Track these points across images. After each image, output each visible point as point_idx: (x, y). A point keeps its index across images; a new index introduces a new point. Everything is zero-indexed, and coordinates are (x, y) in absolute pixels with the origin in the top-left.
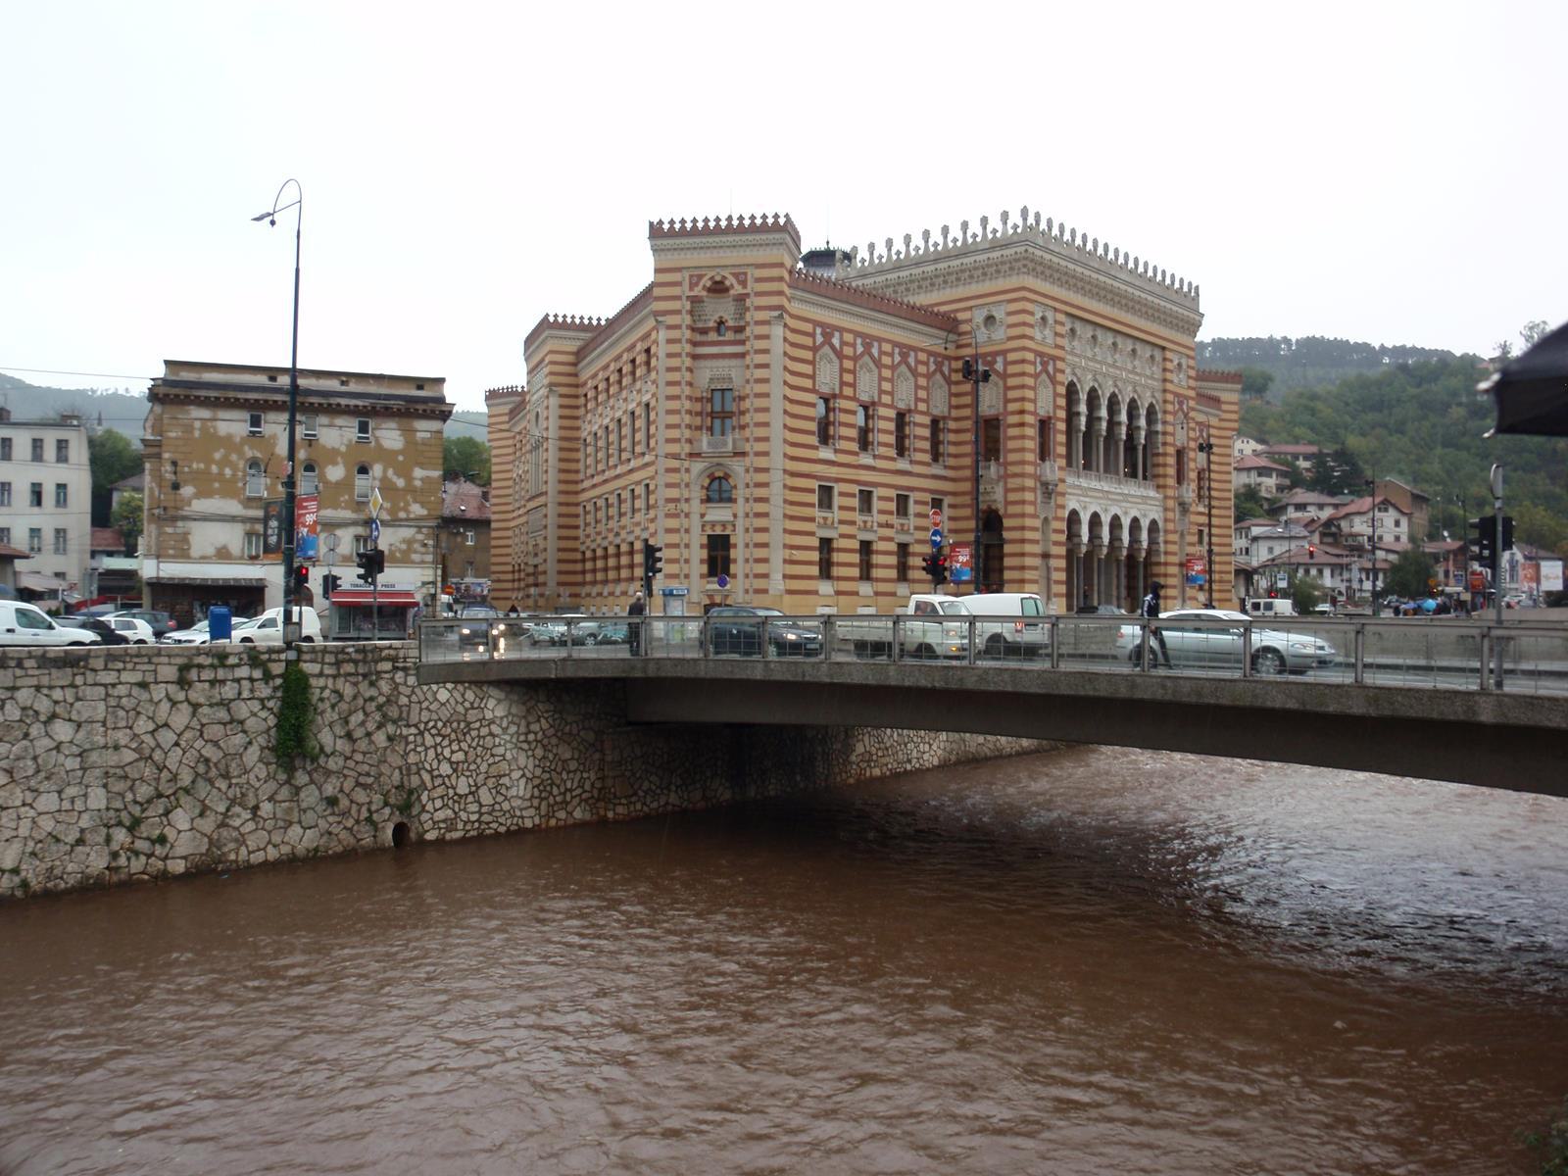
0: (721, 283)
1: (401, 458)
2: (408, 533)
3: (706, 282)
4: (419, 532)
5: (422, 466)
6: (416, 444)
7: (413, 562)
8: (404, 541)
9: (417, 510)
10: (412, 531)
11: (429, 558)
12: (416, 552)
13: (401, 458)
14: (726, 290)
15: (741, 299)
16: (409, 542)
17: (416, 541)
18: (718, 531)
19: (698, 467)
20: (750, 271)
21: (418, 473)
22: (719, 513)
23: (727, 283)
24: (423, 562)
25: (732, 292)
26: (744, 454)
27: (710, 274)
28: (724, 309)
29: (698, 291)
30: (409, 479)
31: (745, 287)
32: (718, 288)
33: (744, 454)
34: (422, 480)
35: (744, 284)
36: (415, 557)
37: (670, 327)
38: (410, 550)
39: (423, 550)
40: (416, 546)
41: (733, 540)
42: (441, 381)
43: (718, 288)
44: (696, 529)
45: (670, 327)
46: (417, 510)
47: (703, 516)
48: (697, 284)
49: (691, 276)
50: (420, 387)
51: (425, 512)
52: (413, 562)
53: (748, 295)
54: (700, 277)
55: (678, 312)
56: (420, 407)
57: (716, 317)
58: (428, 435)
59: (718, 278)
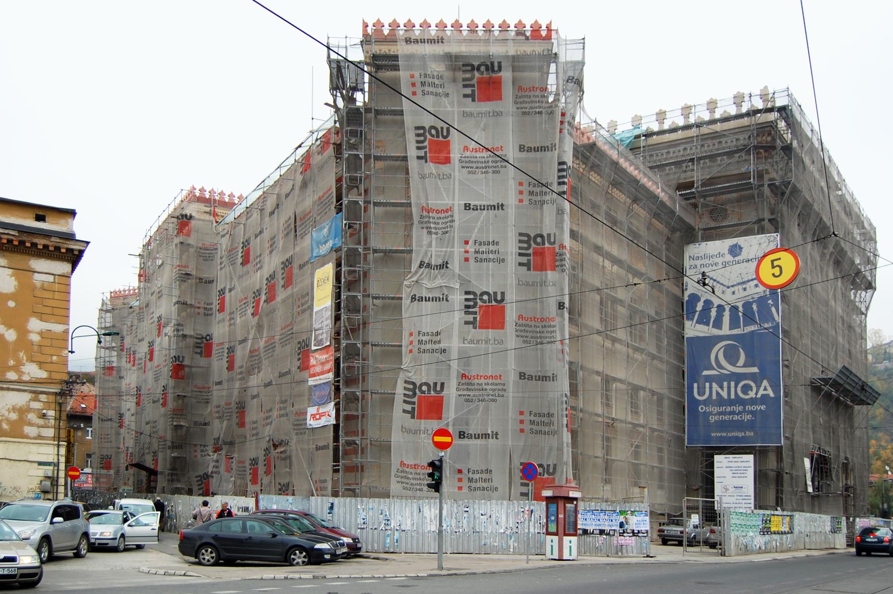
1: (11, 304)
2: (21, 399)
4: (36, 399)
5: (41, 316)
6: (34, 288)
7: (27, 437)
8: (14, 409)
9: (32, 371)
10: (27, 396)
11: (50, 432)
12: (30, 424)
13: (11, 304)
16: (22, 411)
17: (29, 410)
21: (35, 324)
24: (40, 437)
30: (23, 332)
34: (41, 333)
36: (27, 430)
38: (22, 421)
39: (41, 422)
40: (32, 416)
42: (72, 213)
46: (32, 371)
51: (44, 375)
52: (27, 437)
56: (41, 242)
58: (51, 278)
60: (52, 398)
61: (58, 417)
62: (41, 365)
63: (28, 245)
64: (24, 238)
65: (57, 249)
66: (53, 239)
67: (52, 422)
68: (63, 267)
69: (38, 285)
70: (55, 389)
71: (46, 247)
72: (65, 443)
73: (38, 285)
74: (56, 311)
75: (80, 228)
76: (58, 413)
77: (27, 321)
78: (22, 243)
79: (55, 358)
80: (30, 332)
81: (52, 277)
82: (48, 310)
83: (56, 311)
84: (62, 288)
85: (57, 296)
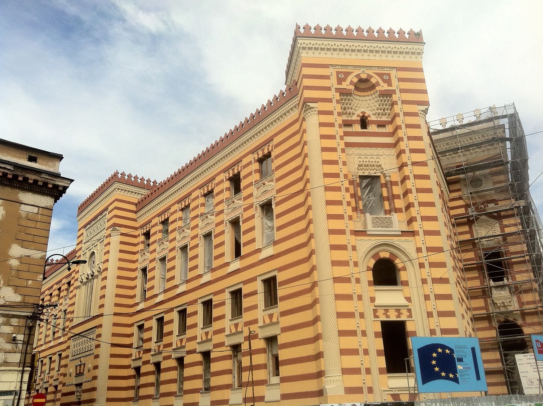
0: (366, 81)
3: (353, 78)
5: (22, 243)
11: (16, 358)
14: (373, 87)
15: (386, 94)
18: (393, 317)
19: (365, 245)
20: (393, 73)
22: (389, 297)
23: (373, 81)
25: (378, 88)
26: (413, 233)
27: (357, 72)
28: (366, 105)
29: (346, 85)
31: (390, 85)
32: (364, 85)
33: (413, 233)
34: (20, 259)
35: (389, 82)
37: (321, 113)
39: (9, 347)
41: (409, 327)
43: (364, 85)
44: (369, 314)
45: (321, 113)
47: (373, 300)
48: (344, 80)
49: (338, 73)
50: (32, 159)
51: (18, 298)
53: (394, 92)
54: (347, 74)
55: (329, 100)
57: (359, 112)
58: (35, 210)
59: (364, 76)
60: (22, 322)
61: (26, 340)
62: (17, 289)
63: (20, 179)
64: (18, 173)
65: (45, 184)
66: (43, 176)
67: (20, 346)
68: (46, 201)
69: (24, 215)
70: (27, 313)
71: (36, 182)
72: (29, 369)
73: (24, 215)
74: (37, 239)
75: (63, 169)
76: (27, 337)
77: (9, 247)
78: (15, 177)
79: (30, 282)
80: (10, 257)
81: (37, 208)
82: (30, 238)
83: (37, 239)
84: (45, 218)
85: (39, 225)
